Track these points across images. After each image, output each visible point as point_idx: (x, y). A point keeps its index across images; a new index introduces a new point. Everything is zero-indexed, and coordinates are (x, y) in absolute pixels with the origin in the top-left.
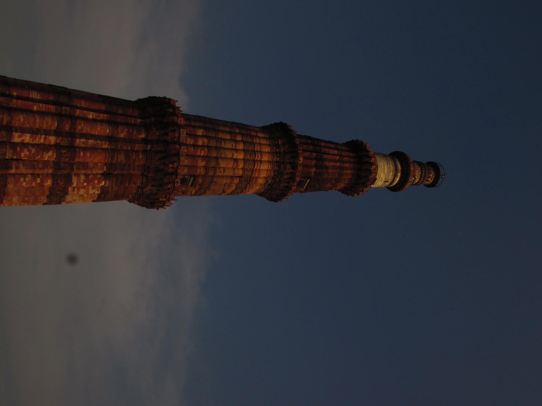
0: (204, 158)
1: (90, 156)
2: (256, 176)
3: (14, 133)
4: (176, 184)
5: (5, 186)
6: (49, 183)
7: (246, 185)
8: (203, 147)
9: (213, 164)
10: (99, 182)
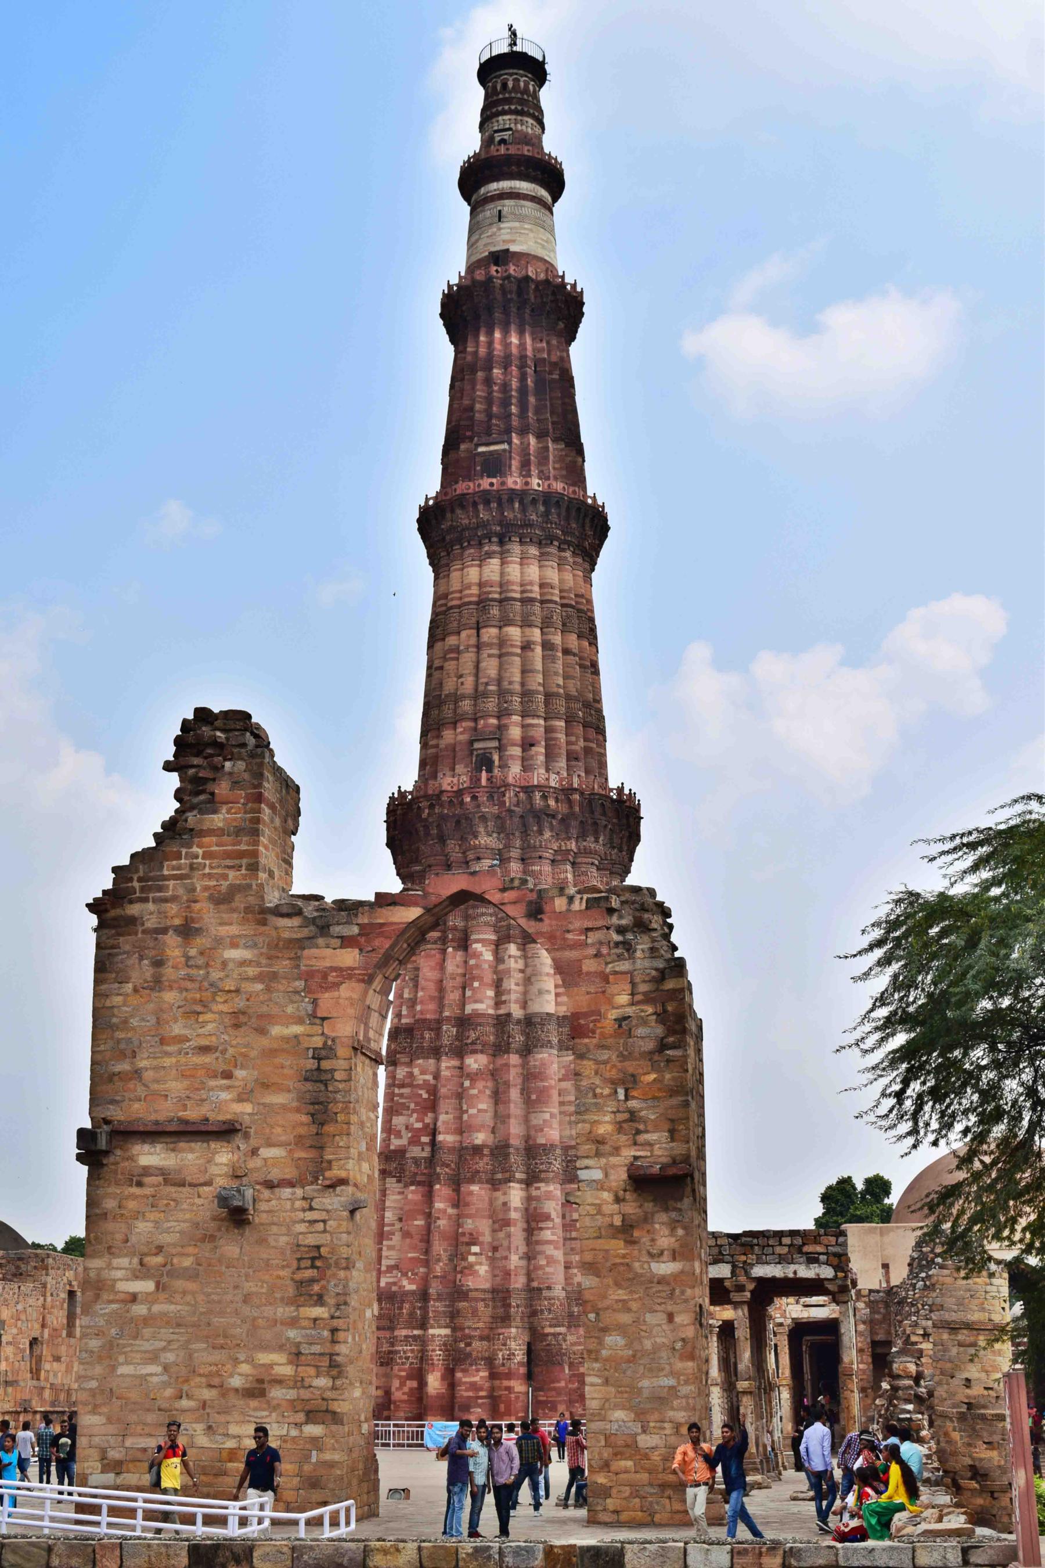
0: (439, 736)
1: (423, 989)
2: (475, 590)
3: (392, 1147)
4: (465, 785)
5: (477, 1150)
6: (475, 1062)
7: (501, 601)
9: (448, 712)
10: (477, 955)
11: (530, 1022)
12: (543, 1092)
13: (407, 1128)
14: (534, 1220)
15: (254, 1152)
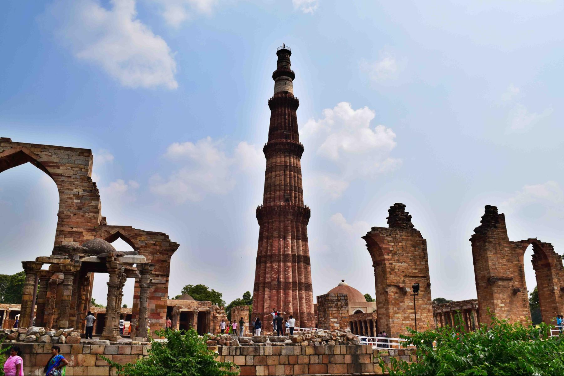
0: (275, 193)
5: (290, 283)
8: (270, 194)
9: (278, 188)
10: (288, 241)
11: (299, 256)
12: (301, 271)
13: (271, 277)
14: (301, 298)
15: (514, 283)
